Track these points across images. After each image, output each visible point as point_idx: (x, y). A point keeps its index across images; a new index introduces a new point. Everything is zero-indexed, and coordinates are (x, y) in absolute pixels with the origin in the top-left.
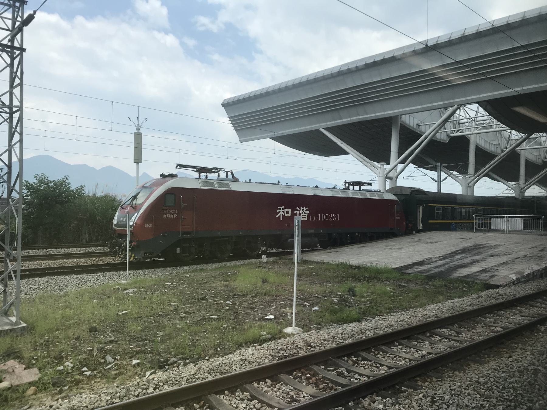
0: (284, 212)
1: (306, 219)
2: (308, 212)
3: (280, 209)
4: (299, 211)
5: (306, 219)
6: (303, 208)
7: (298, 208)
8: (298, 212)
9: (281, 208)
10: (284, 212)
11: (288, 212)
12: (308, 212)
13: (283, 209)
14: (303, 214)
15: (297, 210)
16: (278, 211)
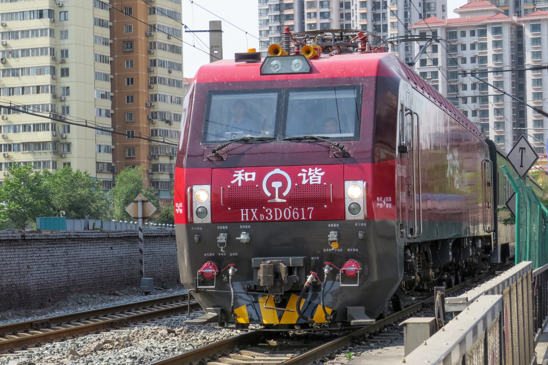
0: (244, 177)
1: (319, 182)
2: (323, 174)
3: (238, 173)
4: (307, 173)
5: (319, 182)
6: (313, 168)
7: (303, 170)
8: (304, 175)
9: (240, 172)
10: (244, 177)
11: (250, 176)
12: (323, 174)
13: (242, 173)
14: (314, 176)
15: (303, 173)
16: (235, 175)
